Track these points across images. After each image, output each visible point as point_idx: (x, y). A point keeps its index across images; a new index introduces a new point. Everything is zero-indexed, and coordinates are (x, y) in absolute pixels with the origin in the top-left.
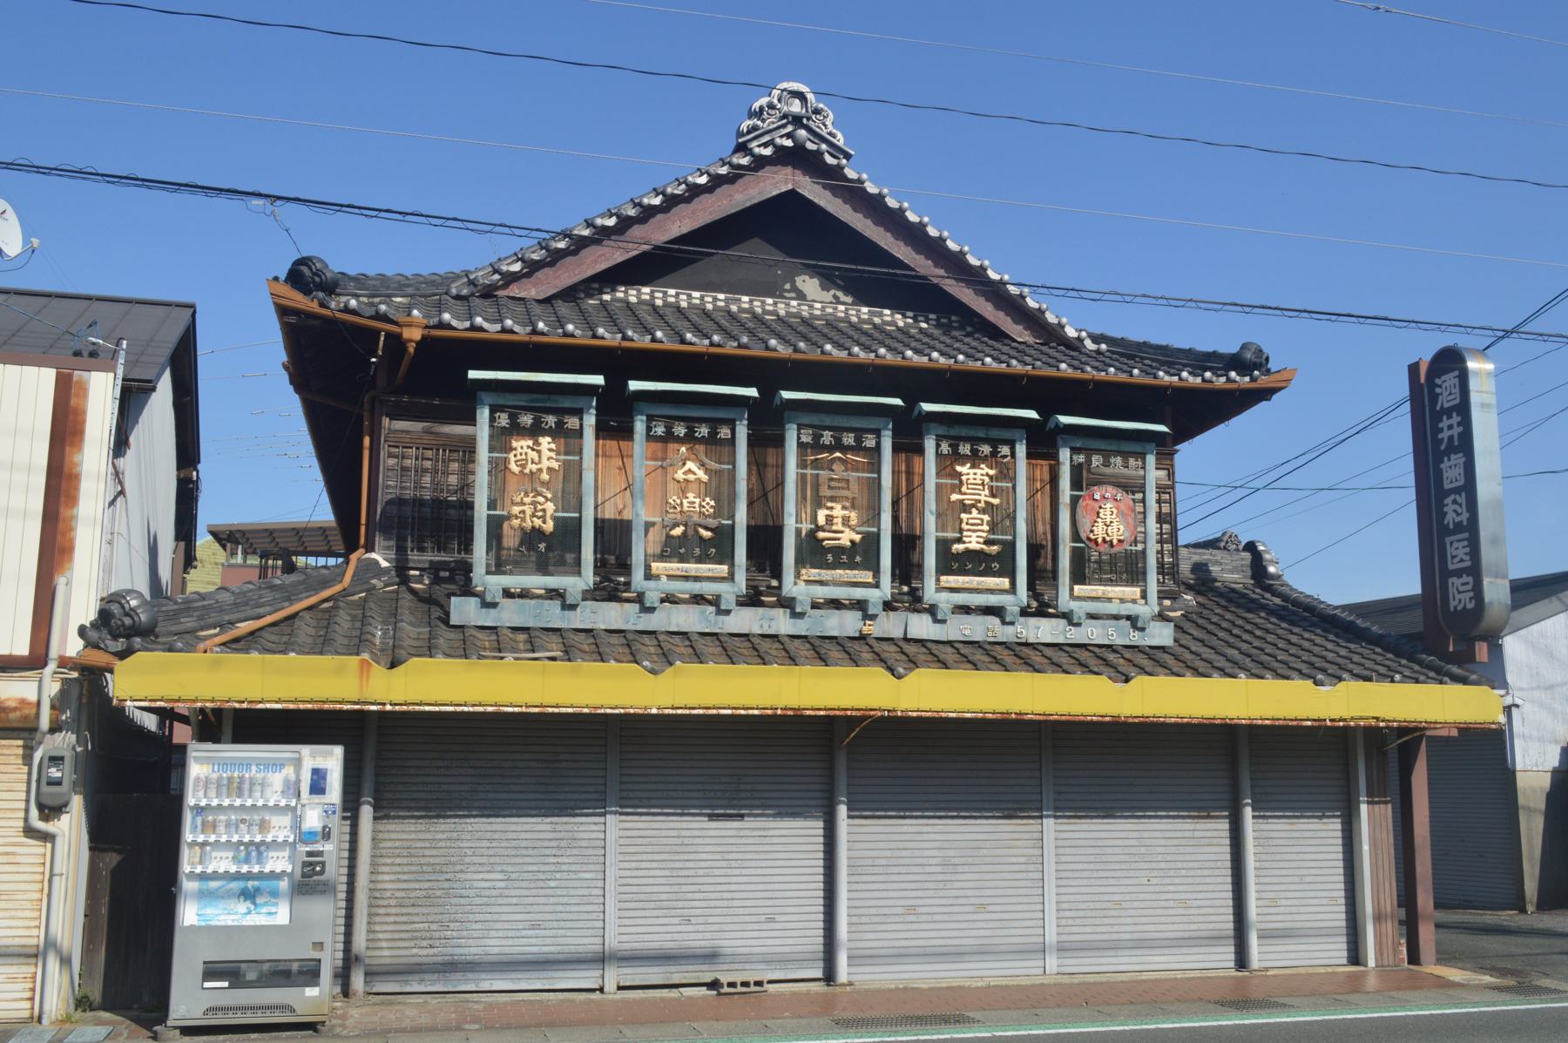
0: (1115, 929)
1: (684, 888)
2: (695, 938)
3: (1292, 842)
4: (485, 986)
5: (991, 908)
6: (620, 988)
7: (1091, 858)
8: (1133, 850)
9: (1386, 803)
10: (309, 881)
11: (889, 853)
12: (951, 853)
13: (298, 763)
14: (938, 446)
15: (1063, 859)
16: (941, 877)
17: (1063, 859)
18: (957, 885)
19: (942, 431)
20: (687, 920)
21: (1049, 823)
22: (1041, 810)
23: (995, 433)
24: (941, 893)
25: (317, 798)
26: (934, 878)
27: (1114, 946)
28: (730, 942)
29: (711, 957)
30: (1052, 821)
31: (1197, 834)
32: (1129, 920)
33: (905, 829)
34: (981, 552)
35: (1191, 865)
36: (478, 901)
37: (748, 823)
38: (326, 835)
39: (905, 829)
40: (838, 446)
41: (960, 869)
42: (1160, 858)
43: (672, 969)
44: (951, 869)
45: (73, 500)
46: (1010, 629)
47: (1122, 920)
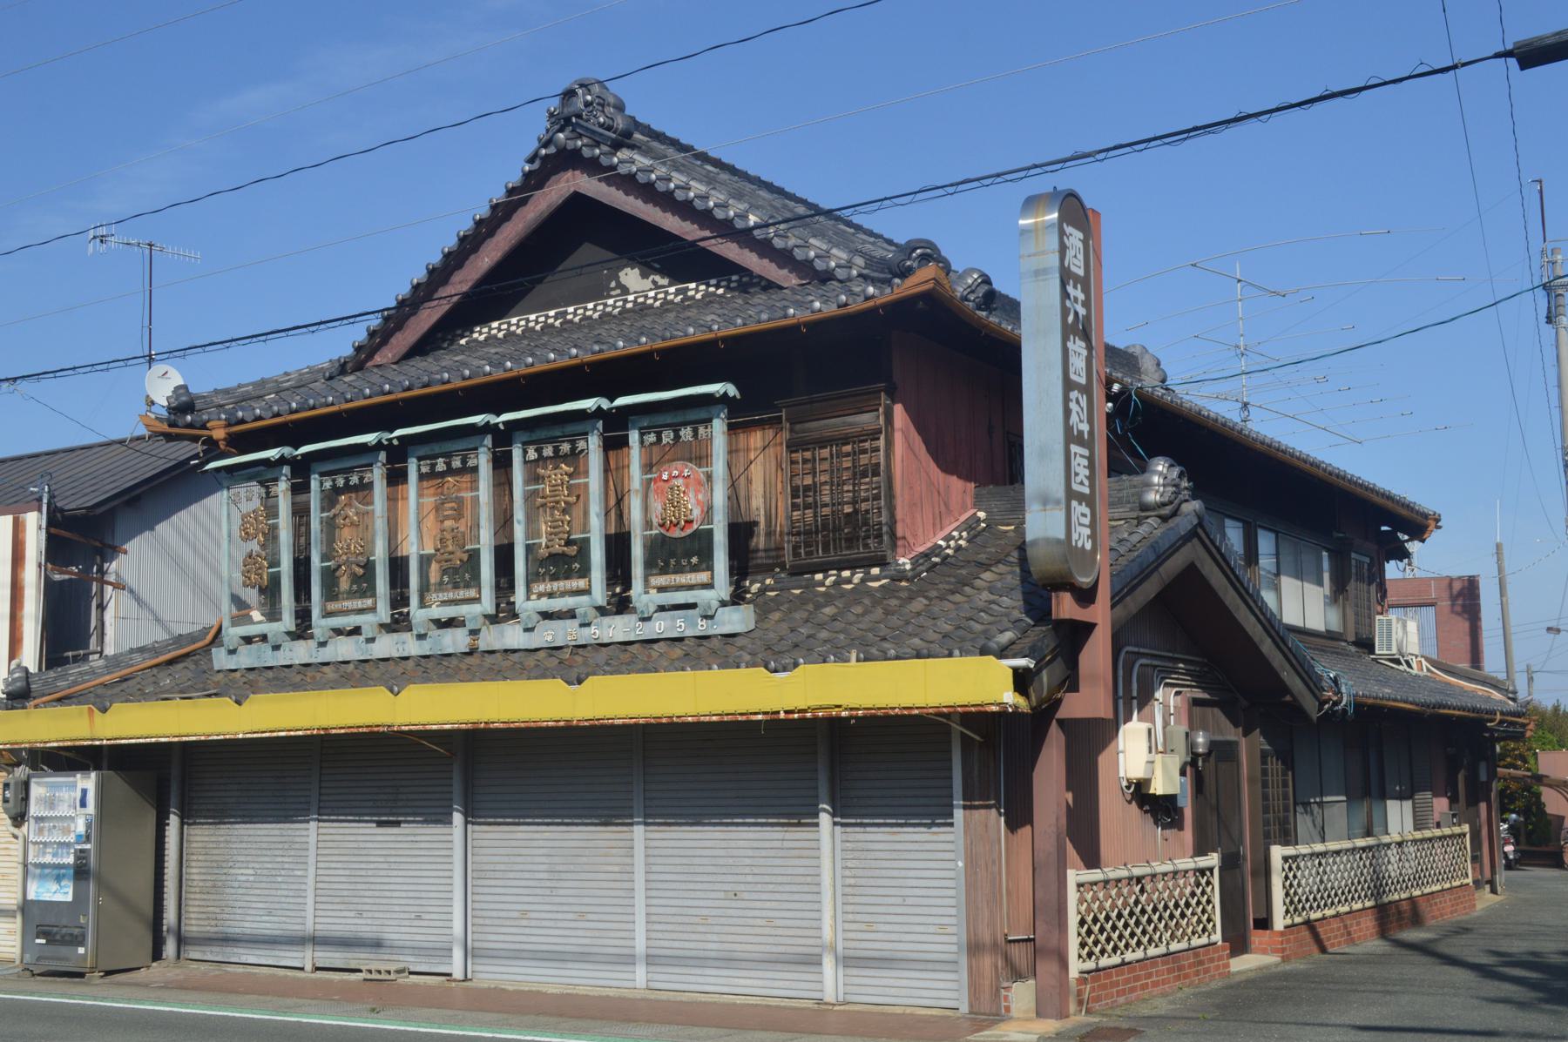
0: (701, 946)
1: (359, 886)
2: (365, 929)
3: (894, 855)
4: (252, 960)
5: (590, 917)
6: (318, 969)
7: (679, 869)
8: (721, 861)
9: (988, 807)
10: (81, 872)
11: (506, 859)
12: (556, 860)
13: (74, 786)
14: (525, 452)
15: (654, 868)
16: (549, 884)
17: (654, 868)
18: (562, 892)
19: (525, 437)
20: (360, 914)
21: (639, 831)
22: (631, 816)
23: (570, 429)
24: (548, 899)
25: (84, 811)
26: (543, 884)
27: (701, 961)
28: (391, 935)
29: (377, 944)
30: (642, 828)
31: (786, 844)
32: (715, 938)
33: (520, 836)
34: (564, 555)
35: (780, 879)
36: (240, 891)
37: (405, 829)
38: (88, 839)
39: (520, 836)
40: (450, 471)
41: (563, 876)
42: (747, 870)
43: (349, 955)
44: (556, 876)
45: (22, 607)
46: (586, 630)
47: (710, 937)
